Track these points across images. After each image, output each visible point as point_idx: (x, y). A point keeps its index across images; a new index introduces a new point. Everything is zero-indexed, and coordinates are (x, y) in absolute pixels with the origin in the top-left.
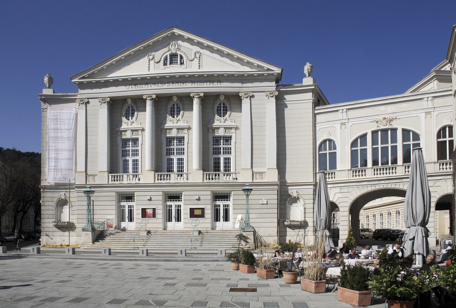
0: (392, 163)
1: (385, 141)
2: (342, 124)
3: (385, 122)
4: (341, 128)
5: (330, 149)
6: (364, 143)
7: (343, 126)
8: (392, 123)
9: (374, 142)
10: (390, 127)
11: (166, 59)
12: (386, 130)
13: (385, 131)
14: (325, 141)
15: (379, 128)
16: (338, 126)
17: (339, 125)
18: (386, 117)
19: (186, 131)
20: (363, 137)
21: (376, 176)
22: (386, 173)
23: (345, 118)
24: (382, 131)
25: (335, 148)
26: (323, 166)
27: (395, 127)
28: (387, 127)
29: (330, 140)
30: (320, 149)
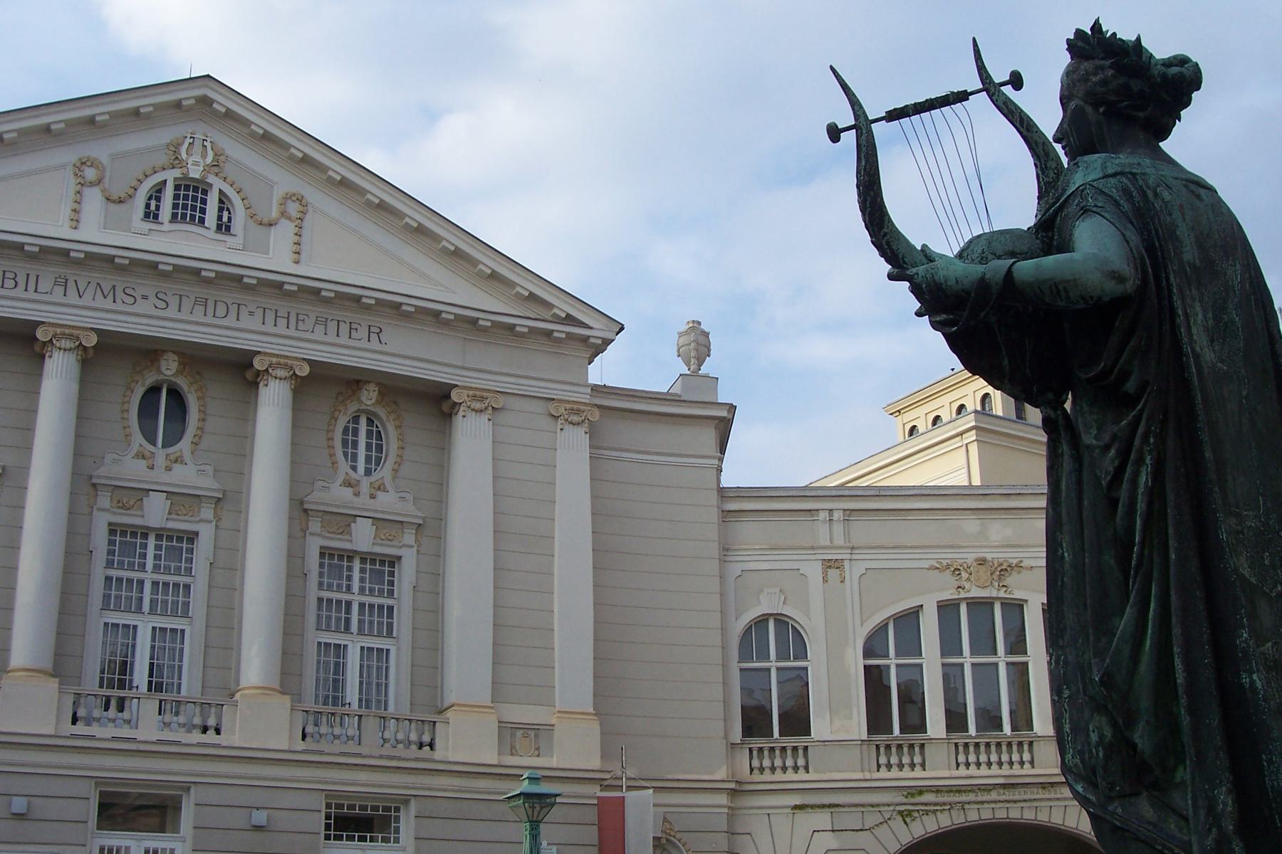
0: (1014, 728)
1: (984, 643)
2: (829, 564)
3: (983, 573)
4: (825, 580)
5: (779, 658)
6: (910, 645)
7: (833, 573)
8: (1008, 581)
9: (950, 644)
10: (1002, 594)
11: (159, 190)
12: (987, 604)
13: (981, 607)
14: (761, 622)
15: (963, 595)
16: (813, 570)
17: (818, 567)
18: (989, 556)
19: (207, 512)
20: (908, 620)
21: (963, 771)
22: (1000, 764)
23: (839, 541)
24: (974, 604)
25: (802, 653)
26: (755, 722)
27: (1018, 595)
28: (994, 594)
29: (782, 621)
30: (745, 654)
